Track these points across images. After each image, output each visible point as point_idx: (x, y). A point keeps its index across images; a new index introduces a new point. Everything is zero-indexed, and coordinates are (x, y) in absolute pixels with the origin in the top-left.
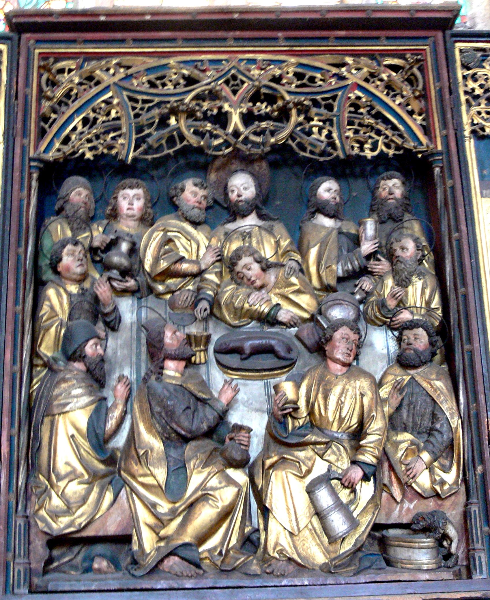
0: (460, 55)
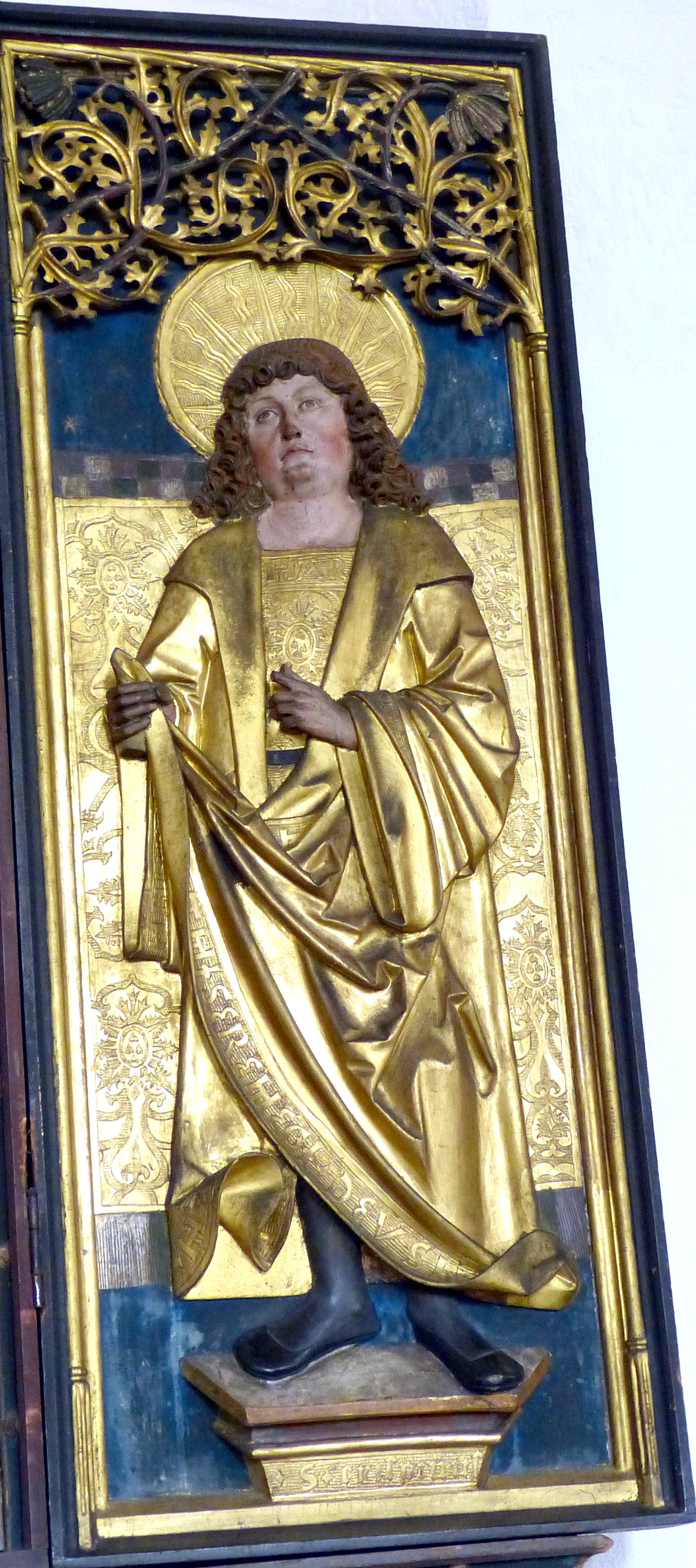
0: (16, 76)
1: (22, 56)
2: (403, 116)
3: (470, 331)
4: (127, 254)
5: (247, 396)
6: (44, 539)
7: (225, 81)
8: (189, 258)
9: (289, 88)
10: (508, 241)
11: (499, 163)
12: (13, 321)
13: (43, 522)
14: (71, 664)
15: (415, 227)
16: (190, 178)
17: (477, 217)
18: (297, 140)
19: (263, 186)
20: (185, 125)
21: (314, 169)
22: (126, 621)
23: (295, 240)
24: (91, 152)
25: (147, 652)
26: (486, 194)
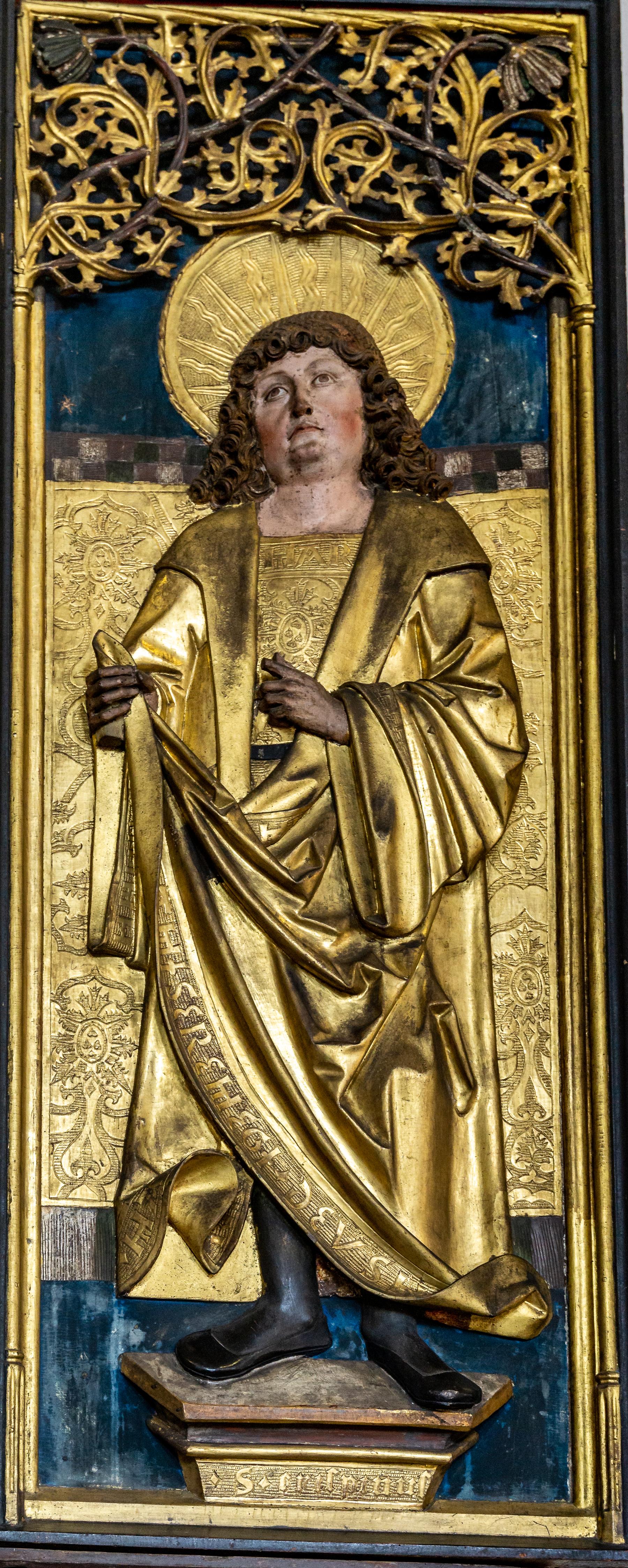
0: (34, 40)
1: (41, 17)
2: (450, 72)
3: (508, 304)
4: (139, 223)
5: (256, 373)
6: (32, 522)
7: (256, 37)
8: (205, 228)
9: (325, 44)
10: (559, 205)
11: (554, 121)
12: (14, 293)
13: (32, 504)
14: (52, 651)
15: (454, 192)
16: (211, 143)
17: (524, 181)
18: (329, 97)
19: (290, 150)
20: (209, 85)
21: (345, 131)
22: (111, 609)
23: (321, 207)
24: (107, 116)
25: (132, 641)
26: (538, 157)
